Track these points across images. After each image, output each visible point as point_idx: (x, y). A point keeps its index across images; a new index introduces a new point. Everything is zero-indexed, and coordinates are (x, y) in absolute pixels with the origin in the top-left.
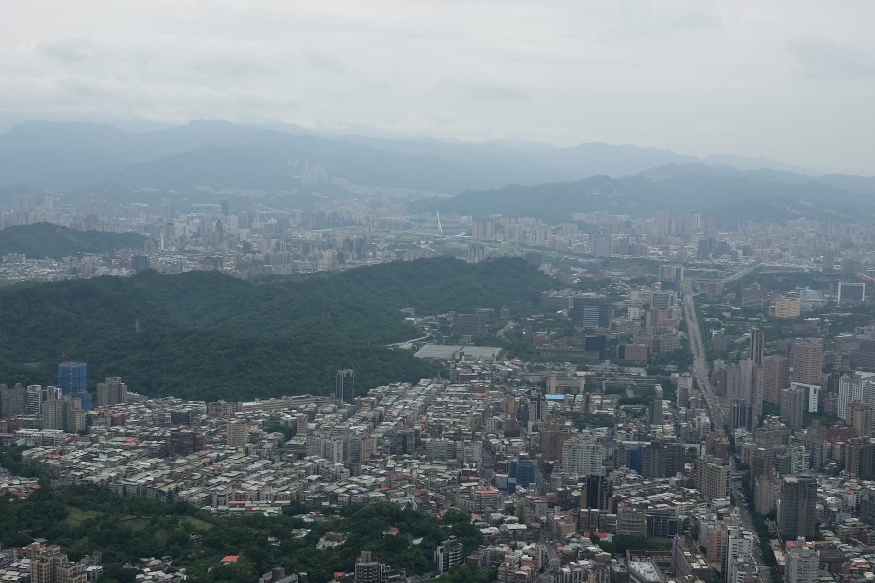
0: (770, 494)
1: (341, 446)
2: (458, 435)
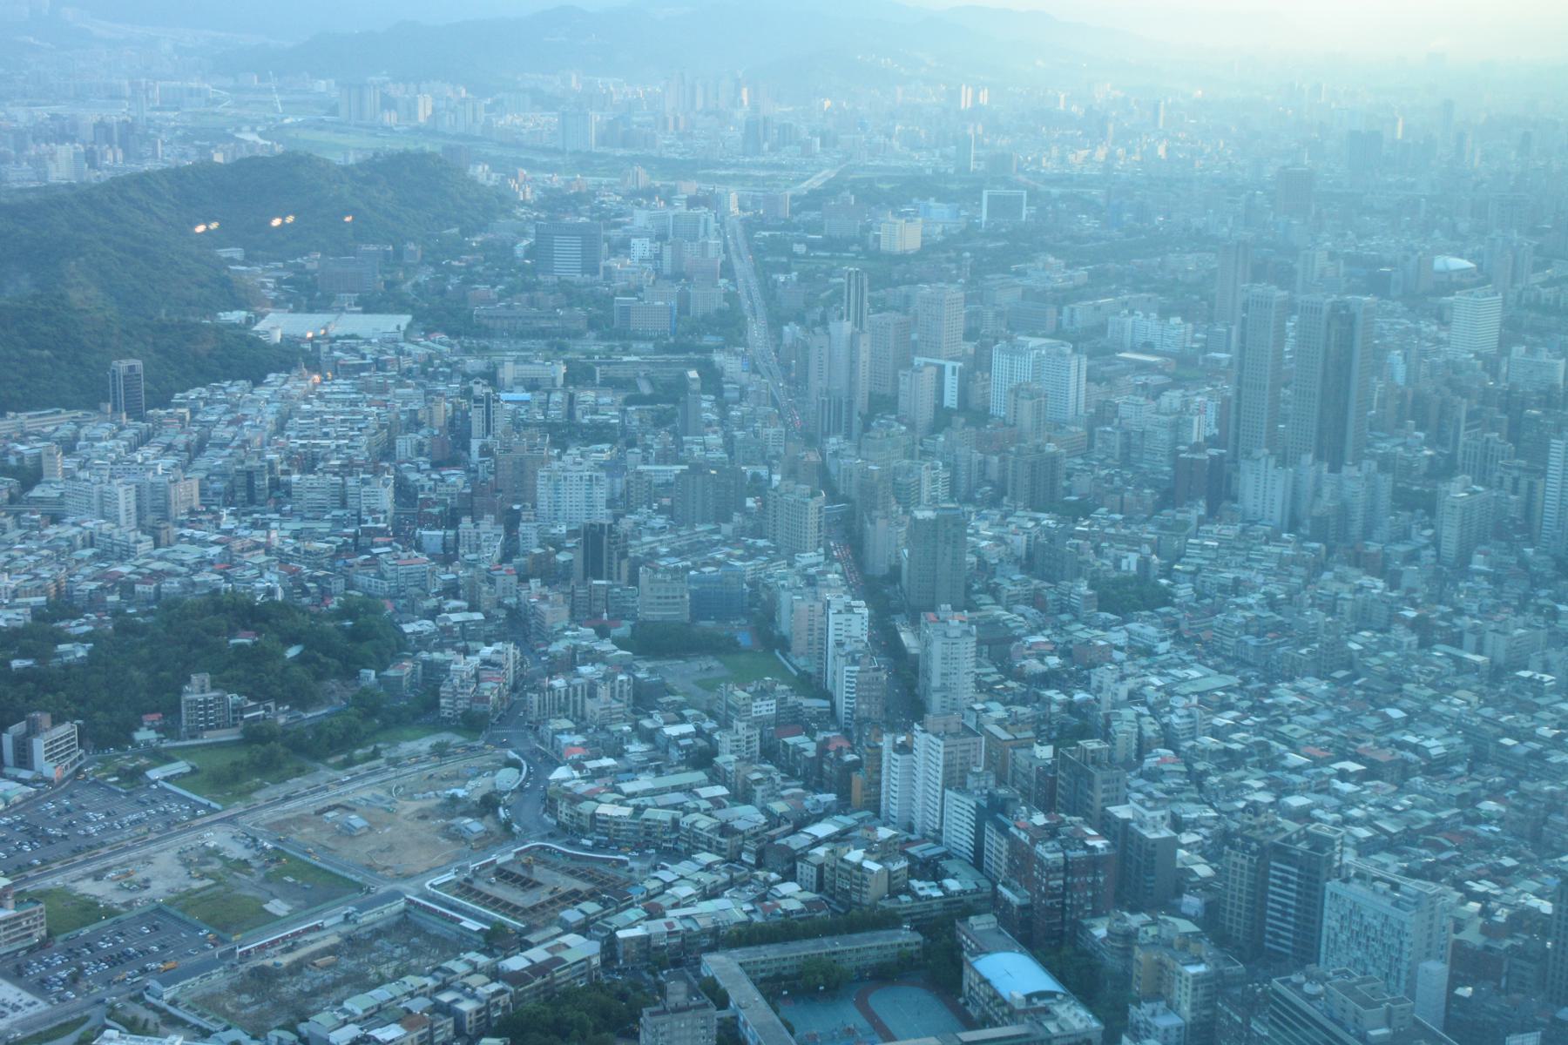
0: (889, 541)
1: (132, 494)
2: (348, 468)
